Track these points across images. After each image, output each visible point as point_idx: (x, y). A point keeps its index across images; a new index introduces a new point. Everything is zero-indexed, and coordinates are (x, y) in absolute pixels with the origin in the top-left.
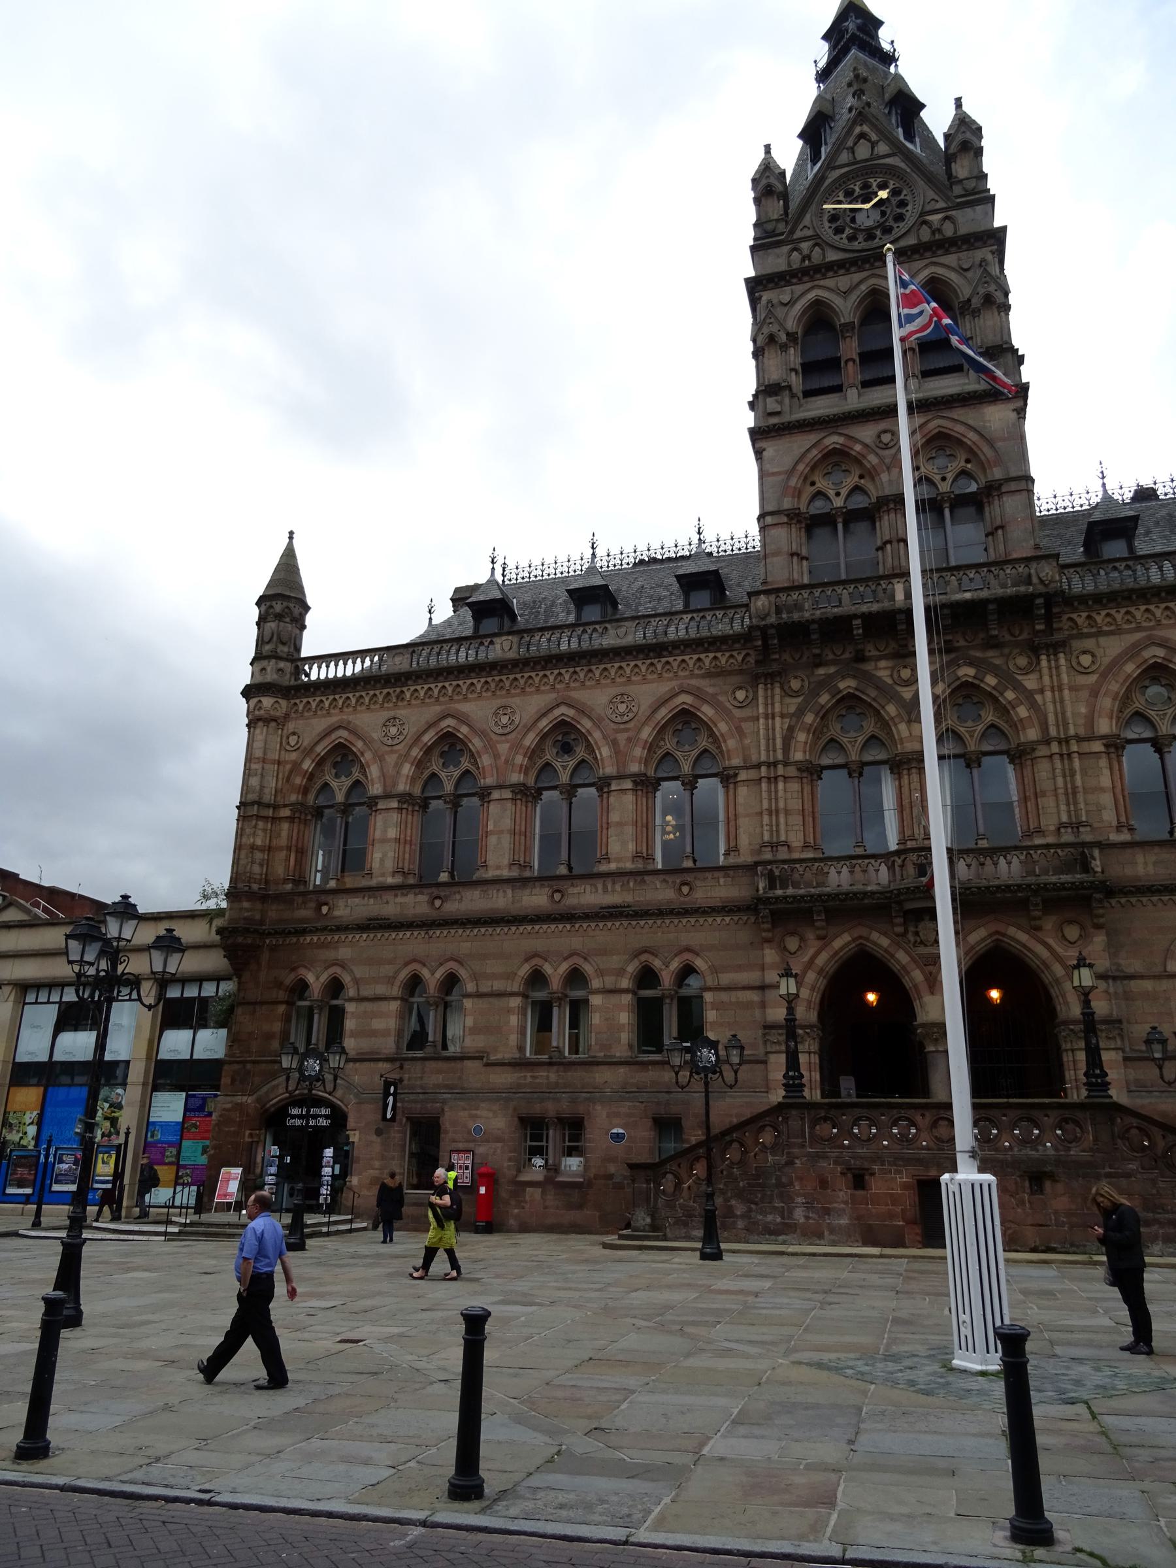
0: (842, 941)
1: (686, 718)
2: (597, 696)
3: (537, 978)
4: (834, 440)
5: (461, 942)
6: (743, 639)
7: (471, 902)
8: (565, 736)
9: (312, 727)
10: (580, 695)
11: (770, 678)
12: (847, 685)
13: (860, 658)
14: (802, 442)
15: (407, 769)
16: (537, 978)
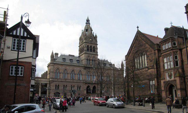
0: (88, 85)
1: (80, 71)
2: (75, 68)
3: (72, 86)
4: (89, 55)
5: (67, 83)
6: (84, 67)
7: (68, 81)
8: (73, 71)
9: (56, 66)
10: (75, 68)
11: (85, 69)
12: (89, 71)
13: (90, 69)
14: (88, 55)
15: (63, 71)
16: (72, 86)
